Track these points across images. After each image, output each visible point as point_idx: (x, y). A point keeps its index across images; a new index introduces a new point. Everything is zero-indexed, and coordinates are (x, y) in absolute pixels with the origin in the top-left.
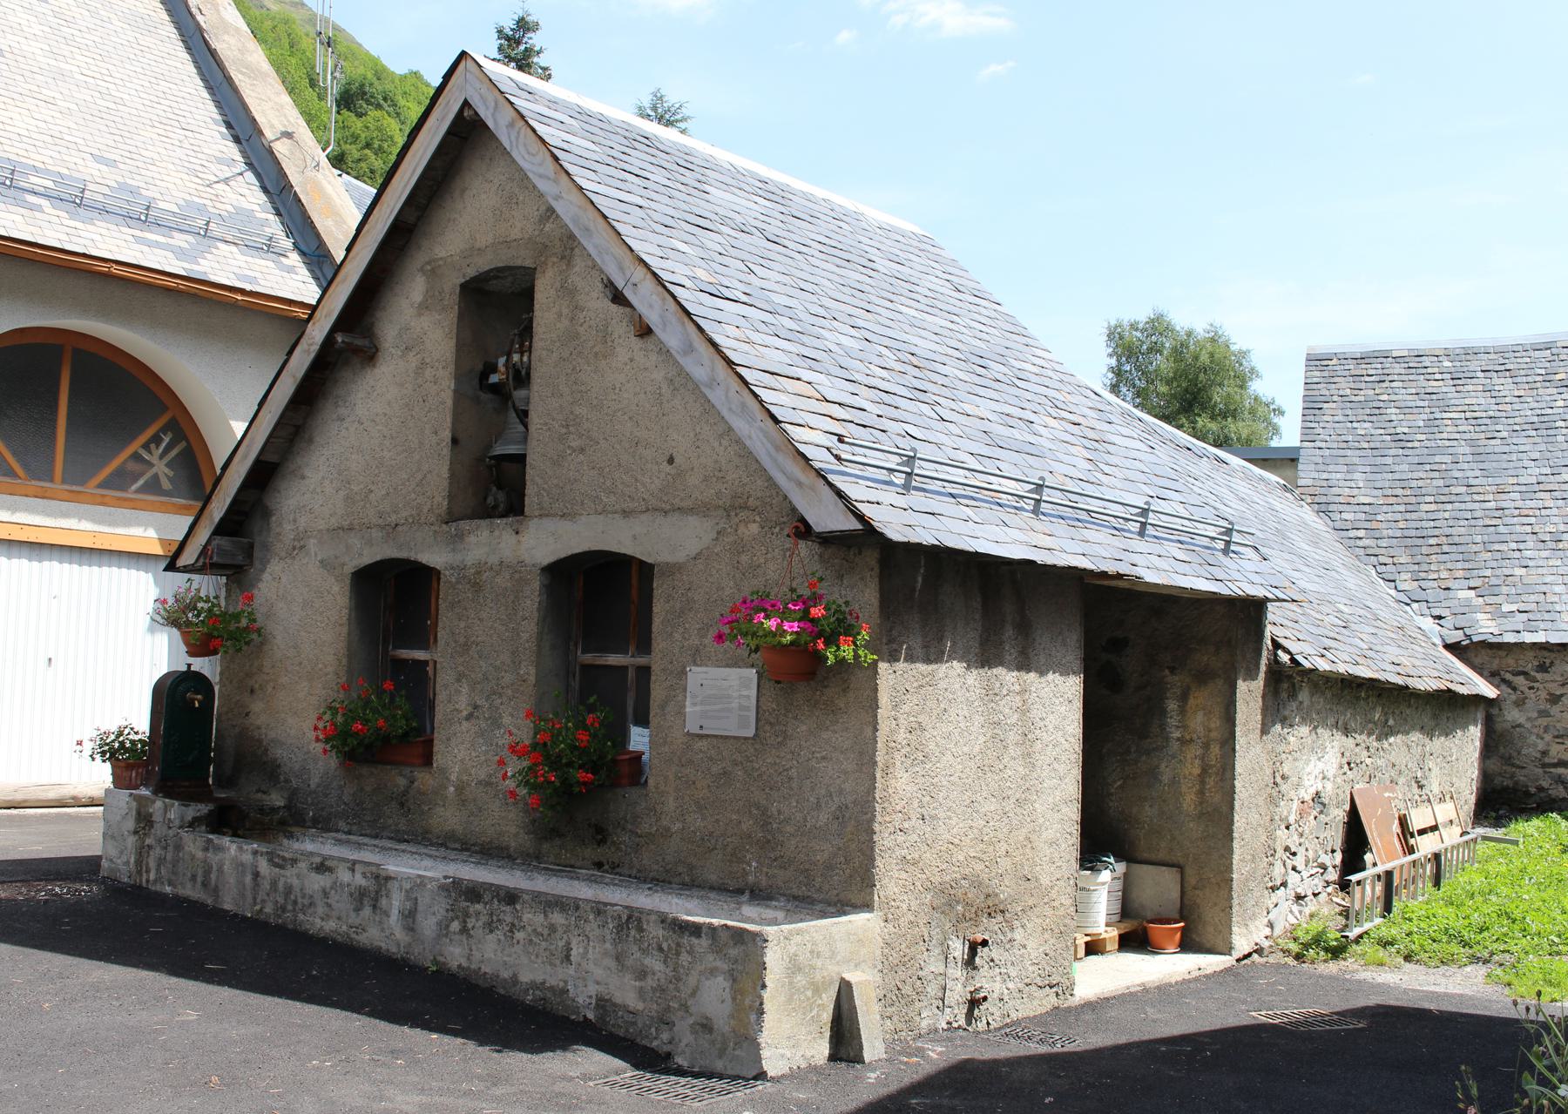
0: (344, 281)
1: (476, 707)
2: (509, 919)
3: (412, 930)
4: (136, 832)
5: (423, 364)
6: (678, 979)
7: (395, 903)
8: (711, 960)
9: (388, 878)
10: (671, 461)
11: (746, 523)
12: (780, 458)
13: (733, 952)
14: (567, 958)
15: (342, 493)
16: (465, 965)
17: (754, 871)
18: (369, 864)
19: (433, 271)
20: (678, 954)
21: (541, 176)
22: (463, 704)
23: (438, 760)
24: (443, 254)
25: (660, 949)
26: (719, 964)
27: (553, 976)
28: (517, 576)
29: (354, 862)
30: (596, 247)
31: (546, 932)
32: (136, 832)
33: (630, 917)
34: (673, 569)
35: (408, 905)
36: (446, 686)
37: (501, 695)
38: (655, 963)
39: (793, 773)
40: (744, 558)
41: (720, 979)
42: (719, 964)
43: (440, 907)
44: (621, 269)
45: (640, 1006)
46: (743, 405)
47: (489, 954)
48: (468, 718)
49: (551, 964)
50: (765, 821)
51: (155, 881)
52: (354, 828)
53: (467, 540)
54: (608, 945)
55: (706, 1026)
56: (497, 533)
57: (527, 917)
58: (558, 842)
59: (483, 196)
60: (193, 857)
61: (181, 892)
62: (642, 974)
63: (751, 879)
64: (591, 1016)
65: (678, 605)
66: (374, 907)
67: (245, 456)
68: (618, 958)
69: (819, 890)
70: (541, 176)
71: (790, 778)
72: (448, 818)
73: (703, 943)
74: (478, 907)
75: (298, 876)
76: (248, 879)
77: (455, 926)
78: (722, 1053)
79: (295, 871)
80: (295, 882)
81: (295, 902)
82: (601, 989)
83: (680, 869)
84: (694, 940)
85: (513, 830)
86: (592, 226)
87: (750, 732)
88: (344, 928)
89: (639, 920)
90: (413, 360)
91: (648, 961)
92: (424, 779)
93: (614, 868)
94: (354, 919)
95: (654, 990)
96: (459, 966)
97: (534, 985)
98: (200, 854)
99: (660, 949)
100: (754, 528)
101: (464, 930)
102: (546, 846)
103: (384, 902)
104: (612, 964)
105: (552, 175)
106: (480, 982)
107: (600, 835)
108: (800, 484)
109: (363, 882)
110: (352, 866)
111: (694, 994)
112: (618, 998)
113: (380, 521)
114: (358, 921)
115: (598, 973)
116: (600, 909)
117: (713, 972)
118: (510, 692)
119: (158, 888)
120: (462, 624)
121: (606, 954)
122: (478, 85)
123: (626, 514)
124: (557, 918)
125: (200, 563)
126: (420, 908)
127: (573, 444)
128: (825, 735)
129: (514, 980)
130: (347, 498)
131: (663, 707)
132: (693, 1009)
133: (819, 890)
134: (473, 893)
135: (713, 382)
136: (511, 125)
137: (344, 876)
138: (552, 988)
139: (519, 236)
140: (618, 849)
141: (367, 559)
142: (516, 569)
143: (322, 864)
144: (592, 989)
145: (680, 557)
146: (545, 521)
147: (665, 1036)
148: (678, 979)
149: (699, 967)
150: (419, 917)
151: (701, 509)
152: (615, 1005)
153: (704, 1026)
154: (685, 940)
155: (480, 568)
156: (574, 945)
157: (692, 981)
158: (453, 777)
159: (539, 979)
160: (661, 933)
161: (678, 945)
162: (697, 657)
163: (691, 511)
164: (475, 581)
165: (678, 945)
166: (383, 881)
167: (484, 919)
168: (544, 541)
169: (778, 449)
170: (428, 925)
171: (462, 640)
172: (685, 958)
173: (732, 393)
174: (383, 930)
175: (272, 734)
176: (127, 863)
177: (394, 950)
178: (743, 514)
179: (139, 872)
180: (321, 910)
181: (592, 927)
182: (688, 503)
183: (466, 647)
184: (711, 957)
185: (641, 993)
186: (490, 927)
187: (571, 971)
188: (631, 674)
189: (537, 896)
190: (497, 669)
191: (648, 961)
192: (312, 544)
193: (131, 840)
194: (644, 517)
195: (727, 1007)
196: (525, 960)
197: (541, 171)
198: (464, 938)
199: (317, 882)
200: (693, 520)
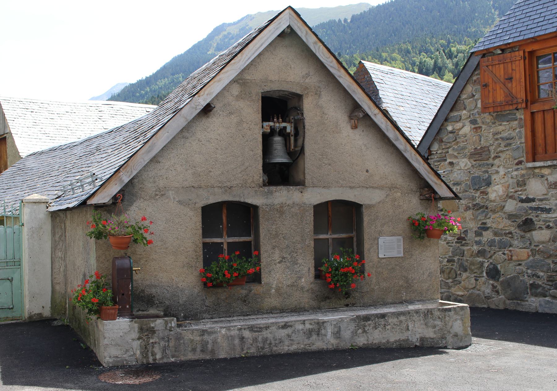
0: (219, 81)
1: (284, 258)
2: (383, 323)
3: (339, 338)
4: (139, 339)
5: (240, 122)
6: (446, 325)
7: (329, 330)
8: (455, 317)
9: (323, 323)
10: (367, 171)
11: (396, 192)
12: (430, 176)
13: (461, 313)
14: (408, 329)
15: (190, 172)
16: (366, 342)
17: (404, 296)
18: (312, 320)
19: (244, 83)
20: (445, 318)
21: (331, 67)
22: (277, 256)
23: (264, 280)
24: (249, 78)
25: (439, 318)
26: (457, 317)
27: (402, 336)
28: (302, 208)
29: (304, 321)
30: (359, 98)
31: (398, 323)
32: (139, 339)
33: (428, 311)
34: (370, 206)
35: (336, 330)
36: (266, 251)
37: (296, 253)
38: (438, 322)
39: (415, 265)
40: (396, 203)
41: (458, 321)
42: (457, 317)
43: (352, 327)
44: (370, 108)
45: (435, 336)
46: (417, 159)
47: (377, 336)
48: (279, 263)
49: (402, 333)
50: (407, 280)
51: (162, 358)
52: (215, 316)
53: (274, 194)
54: (422, 322)
55: (456, 335)
56: (291, 192)
57: (390, 320)
58: (328, 301)
59: (272, 60)
60: (192, 341)
61: (183, 358)
62: (434, 327)
63: (404, 298)
64: (418, 344)
65: (373, 218)
66: (318, 334)
67: (148, 152)
68: (426, 325)
69: (425, 297)
70: (331, 67)
71: (414, 267)
72: (273, 301)
73: (453, 312)
74: (369, 322)
75: (271, 333)
76: (237, 341)
77: (360, 331)
78: (461, 341)
79: (268, 331)
80: (269, 336)
81: (270, 344)
82: (421, 335)
83: (379, 300)
84: (449, 313)
85: (307, 300)
86: (356, 90)
87: (402, 255)
88: (302, 346)
89: (431, 311)
90: (234, 119)
91: (436, 322)
92: (256, 289)
93: (353, 305)
94: (307, 342)
95: (439, 330)
96: (364, 344)
97: (396, 341)
98: (198, 338)
99: (439, 318)
100: (399, 194)
101: (364, 331)
102: (322, 303)
103: (323, 332)
104: (424, 327)
105: (337, 68)
106: (374, 347)
107: (347, 295)
108: (436, 183)
109: (311, 327)
110: (304, 322)
111: (451, 327)
112: (427, 336)
113: (220, 185)
114: (309, 342)
115: (420, 330)
116: (417, 312)
117: (456, 320)
118: (301, 251)
119: (165, 360)
120: (274, 227)
121: (421, 324)
122: (296, 22)
123: (351, 188)
124: (402, 318)
125: (111, 202)
126: (342, 329)
127: (326, 162)
128: (424, 253)
129: (388, 342)
130: (194, 174)
131: (369, 250)
132: (452, 332)
133: (425, 297)
134: (367, 318)
135: (406, 150)
136: (315, 43)
137: (301, 327)
138: (403, 340)
139: (293, 80)
140: (355, 299)
141: (212, 200)
142: (302, 206)
143: (285, 325)
144: (418, 336)
145: (373, 202)
146: (315, 189)
147: (444, 342)
148: (446, 325)
149: (452, 320)
150: (342, 333)
151: (381, 188)
152: (427, 338)
153: (455, 335)
154: (447, 313)
155: (282, 205)
156: (410, 325)
157: (450, 324)
158: (274, 286)
159: (397, 338)
160: (439, 313)
161: (445, 315)
162: (381, 233)
163: (377, 188)
164: (281, 210)
165: (445, 315)
166: (321, 325)
167: (372, 326)
168: (314, 196)
169: (429, 173)
170: (346, 334)
171: (274, 233)
172: (447, 318)
173: (413, 155)
174: (324, 342)
175: (148, 283)
176: (135, 354)
177: (331, 347)
178: (396, 190)
179: (147, 357)
180: (287, 343)
181: (416, 317)
182: (375, 185)
183: (277, 235)
184: (455, 316)
185: (435, 332)
186: (375, 328)
187: (410, 333)
188: (330, 241)
189: (393, 314)
190: (293, 243)
191: (436, 322)
192: (171, 193)
193: (136, 344)
194: (358, 189)
195: (461, 329)
196: (391, 334)
197: (331, 65)
198: (364, 334)
199: (283, 333)
200: (377, 191)
